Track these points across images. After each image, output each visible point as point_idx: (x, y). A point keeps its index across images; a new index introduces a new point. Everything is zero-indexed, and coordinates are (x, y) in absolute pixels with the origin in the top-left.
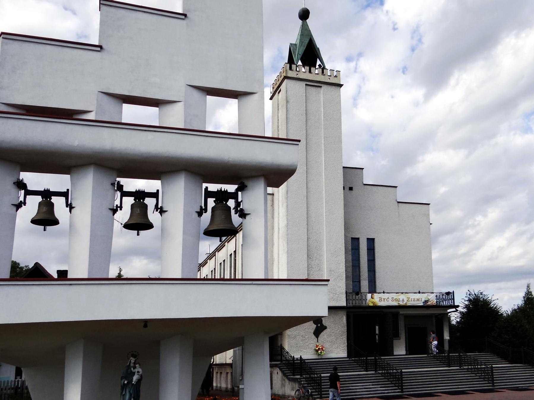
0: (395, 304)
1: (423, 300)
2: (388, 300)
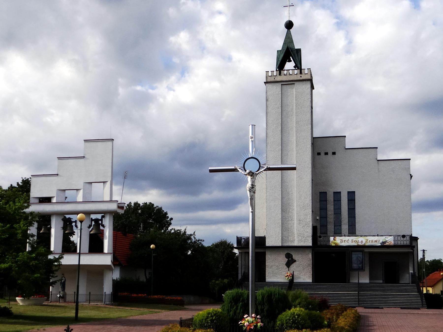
0: (355, 244)
1: (381, 241)
2: (348, 241)
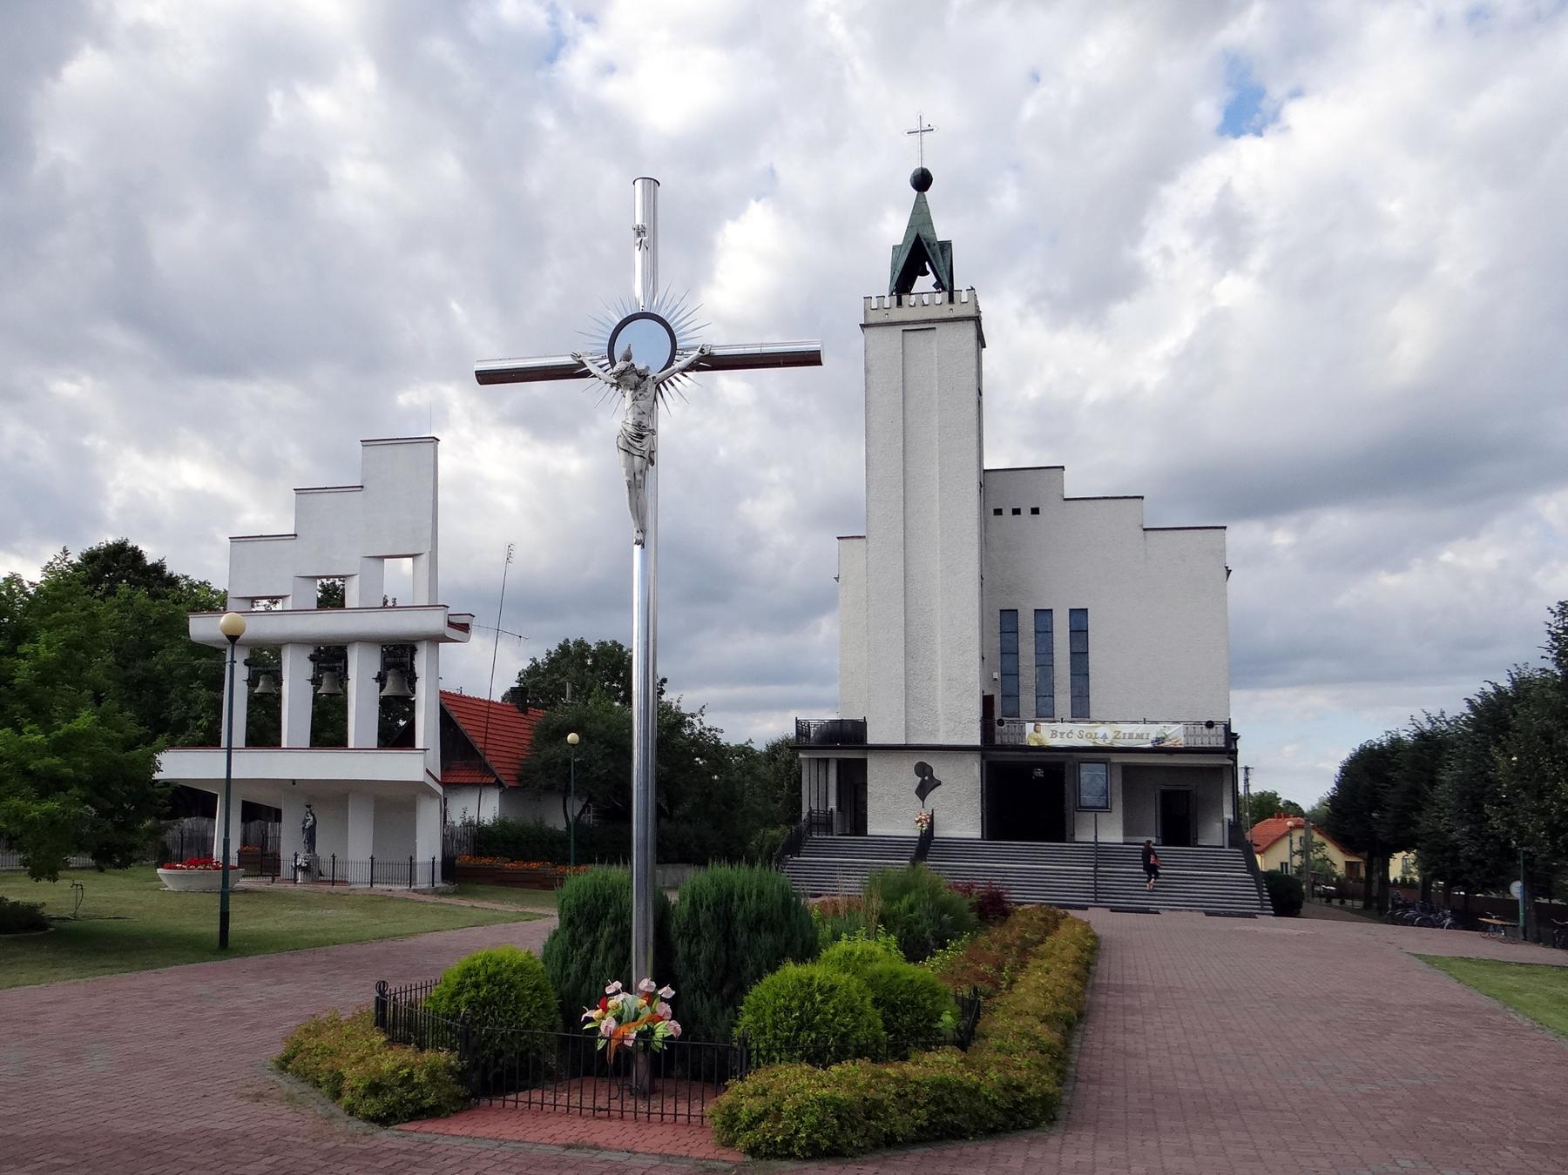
1: (1153, 736)
